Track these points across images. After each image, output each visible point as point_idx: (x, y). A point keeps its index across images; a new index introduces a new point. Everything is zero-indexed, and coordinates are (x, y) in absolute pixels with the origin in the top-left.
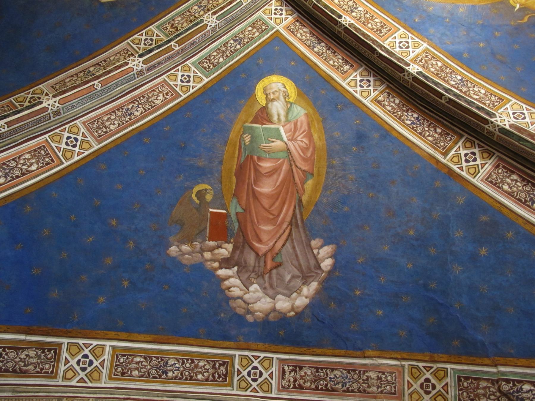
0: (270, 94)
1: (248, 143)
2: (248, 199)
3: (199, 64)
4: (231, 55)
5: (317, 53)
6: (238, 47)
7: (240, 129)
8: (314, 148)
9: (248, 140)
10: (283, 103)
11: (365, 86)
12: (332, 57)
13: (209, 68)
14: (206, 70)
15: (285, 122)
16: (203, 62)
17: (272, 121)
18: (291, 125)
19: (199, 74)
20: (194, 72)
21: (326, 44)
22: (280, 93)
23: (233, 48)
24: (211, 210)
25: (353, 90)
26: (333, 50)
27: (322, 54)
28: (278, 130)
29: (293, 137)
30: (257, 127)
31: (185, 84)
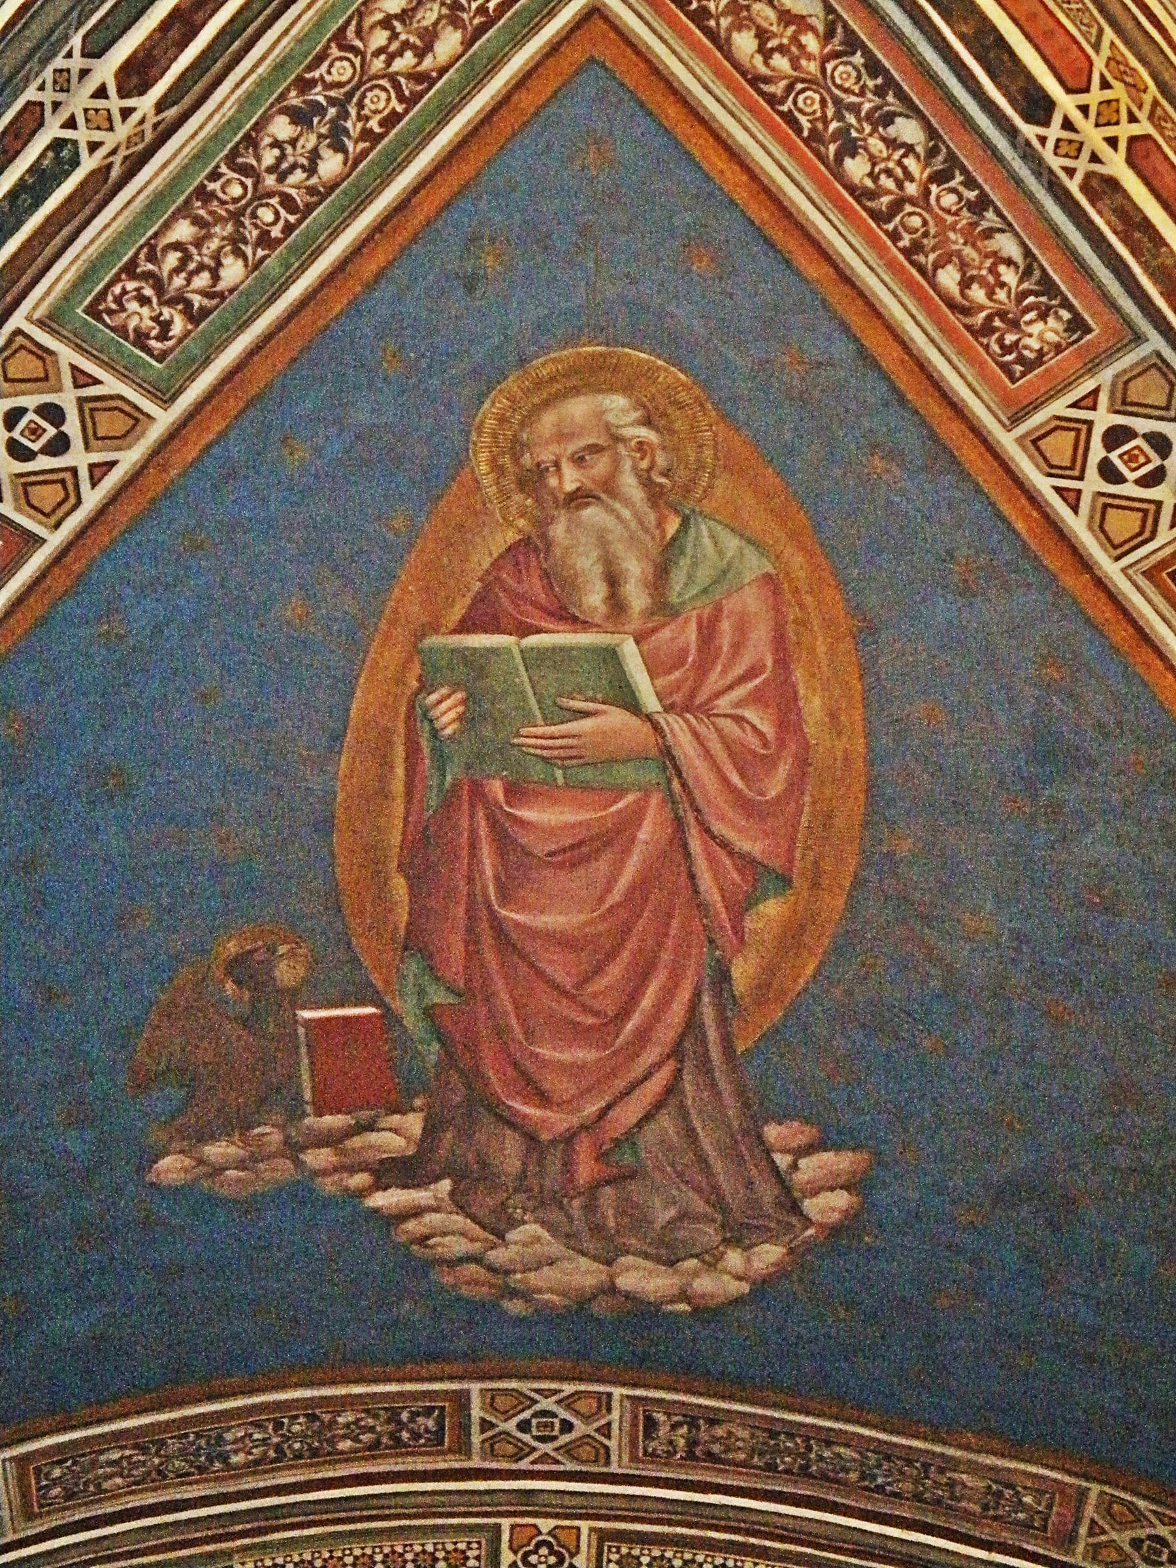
0: (557, 464)
1: (455, 726)
2: (472, 954)
3: (97, 316)
4: (289, 229)
5: (861, 194)
6: (331, 165)
7: (404, 667)
8: (802, 763)
9: (452, 715)
10: (636, 514)
11: (1131, 476)
12: (956, 240)
13: (163, 336)
14: (149, 351)
15: (649, 613)
16: (118, 300)
17: (574, 610)
18: (682, 630)
19: (111, 385)
20: (81, 379)
21: (932, 133)
22: (616, 463)
23: (298, 176)
24: (307, 1014)
25: (1058, 490)
26: (970, 183)
27: (896, 206)
28: (611, 656)
29: (692, 695)
30: (494, 651)
31: (44, 462)
